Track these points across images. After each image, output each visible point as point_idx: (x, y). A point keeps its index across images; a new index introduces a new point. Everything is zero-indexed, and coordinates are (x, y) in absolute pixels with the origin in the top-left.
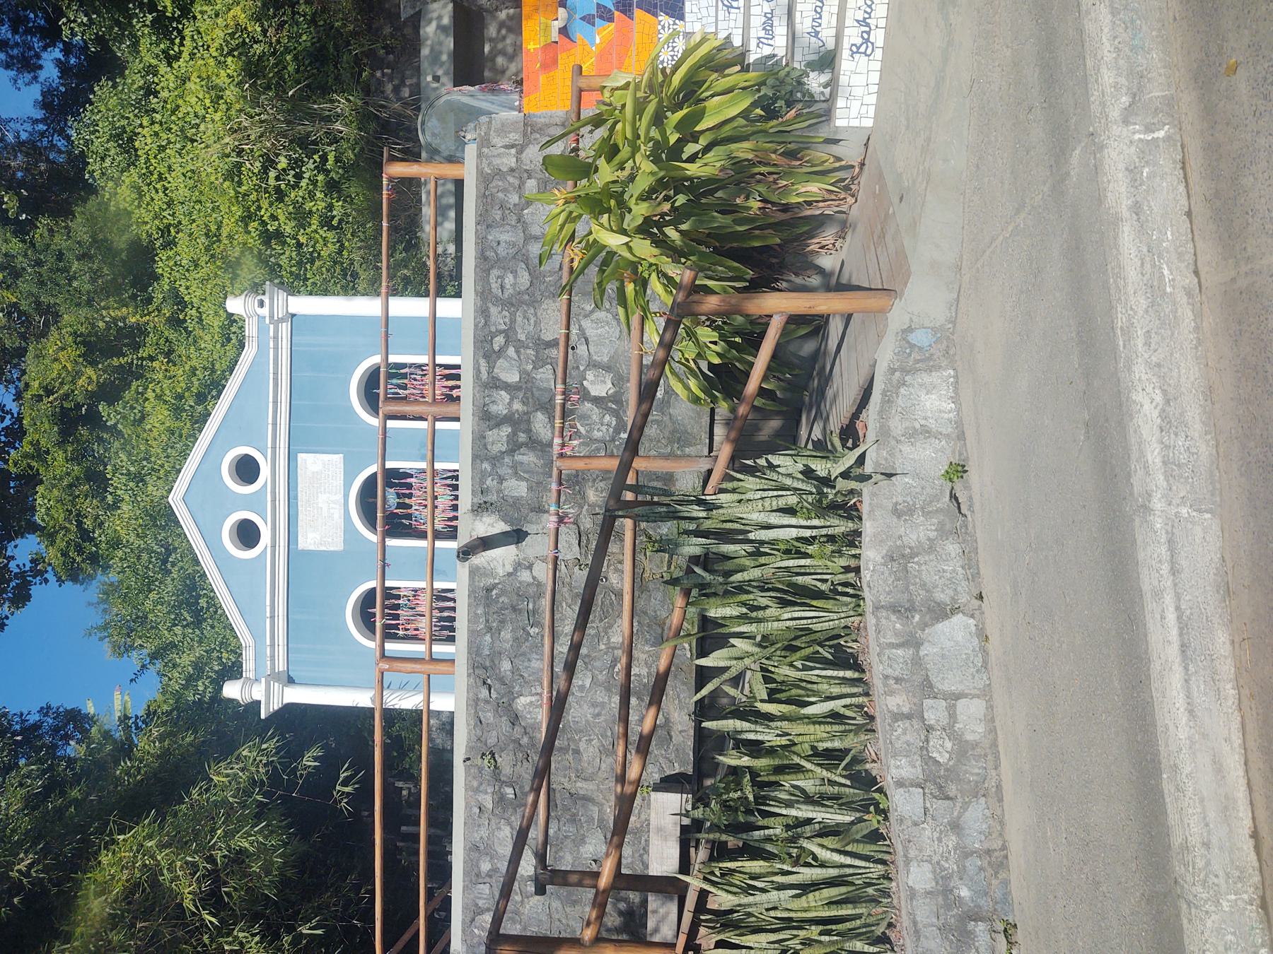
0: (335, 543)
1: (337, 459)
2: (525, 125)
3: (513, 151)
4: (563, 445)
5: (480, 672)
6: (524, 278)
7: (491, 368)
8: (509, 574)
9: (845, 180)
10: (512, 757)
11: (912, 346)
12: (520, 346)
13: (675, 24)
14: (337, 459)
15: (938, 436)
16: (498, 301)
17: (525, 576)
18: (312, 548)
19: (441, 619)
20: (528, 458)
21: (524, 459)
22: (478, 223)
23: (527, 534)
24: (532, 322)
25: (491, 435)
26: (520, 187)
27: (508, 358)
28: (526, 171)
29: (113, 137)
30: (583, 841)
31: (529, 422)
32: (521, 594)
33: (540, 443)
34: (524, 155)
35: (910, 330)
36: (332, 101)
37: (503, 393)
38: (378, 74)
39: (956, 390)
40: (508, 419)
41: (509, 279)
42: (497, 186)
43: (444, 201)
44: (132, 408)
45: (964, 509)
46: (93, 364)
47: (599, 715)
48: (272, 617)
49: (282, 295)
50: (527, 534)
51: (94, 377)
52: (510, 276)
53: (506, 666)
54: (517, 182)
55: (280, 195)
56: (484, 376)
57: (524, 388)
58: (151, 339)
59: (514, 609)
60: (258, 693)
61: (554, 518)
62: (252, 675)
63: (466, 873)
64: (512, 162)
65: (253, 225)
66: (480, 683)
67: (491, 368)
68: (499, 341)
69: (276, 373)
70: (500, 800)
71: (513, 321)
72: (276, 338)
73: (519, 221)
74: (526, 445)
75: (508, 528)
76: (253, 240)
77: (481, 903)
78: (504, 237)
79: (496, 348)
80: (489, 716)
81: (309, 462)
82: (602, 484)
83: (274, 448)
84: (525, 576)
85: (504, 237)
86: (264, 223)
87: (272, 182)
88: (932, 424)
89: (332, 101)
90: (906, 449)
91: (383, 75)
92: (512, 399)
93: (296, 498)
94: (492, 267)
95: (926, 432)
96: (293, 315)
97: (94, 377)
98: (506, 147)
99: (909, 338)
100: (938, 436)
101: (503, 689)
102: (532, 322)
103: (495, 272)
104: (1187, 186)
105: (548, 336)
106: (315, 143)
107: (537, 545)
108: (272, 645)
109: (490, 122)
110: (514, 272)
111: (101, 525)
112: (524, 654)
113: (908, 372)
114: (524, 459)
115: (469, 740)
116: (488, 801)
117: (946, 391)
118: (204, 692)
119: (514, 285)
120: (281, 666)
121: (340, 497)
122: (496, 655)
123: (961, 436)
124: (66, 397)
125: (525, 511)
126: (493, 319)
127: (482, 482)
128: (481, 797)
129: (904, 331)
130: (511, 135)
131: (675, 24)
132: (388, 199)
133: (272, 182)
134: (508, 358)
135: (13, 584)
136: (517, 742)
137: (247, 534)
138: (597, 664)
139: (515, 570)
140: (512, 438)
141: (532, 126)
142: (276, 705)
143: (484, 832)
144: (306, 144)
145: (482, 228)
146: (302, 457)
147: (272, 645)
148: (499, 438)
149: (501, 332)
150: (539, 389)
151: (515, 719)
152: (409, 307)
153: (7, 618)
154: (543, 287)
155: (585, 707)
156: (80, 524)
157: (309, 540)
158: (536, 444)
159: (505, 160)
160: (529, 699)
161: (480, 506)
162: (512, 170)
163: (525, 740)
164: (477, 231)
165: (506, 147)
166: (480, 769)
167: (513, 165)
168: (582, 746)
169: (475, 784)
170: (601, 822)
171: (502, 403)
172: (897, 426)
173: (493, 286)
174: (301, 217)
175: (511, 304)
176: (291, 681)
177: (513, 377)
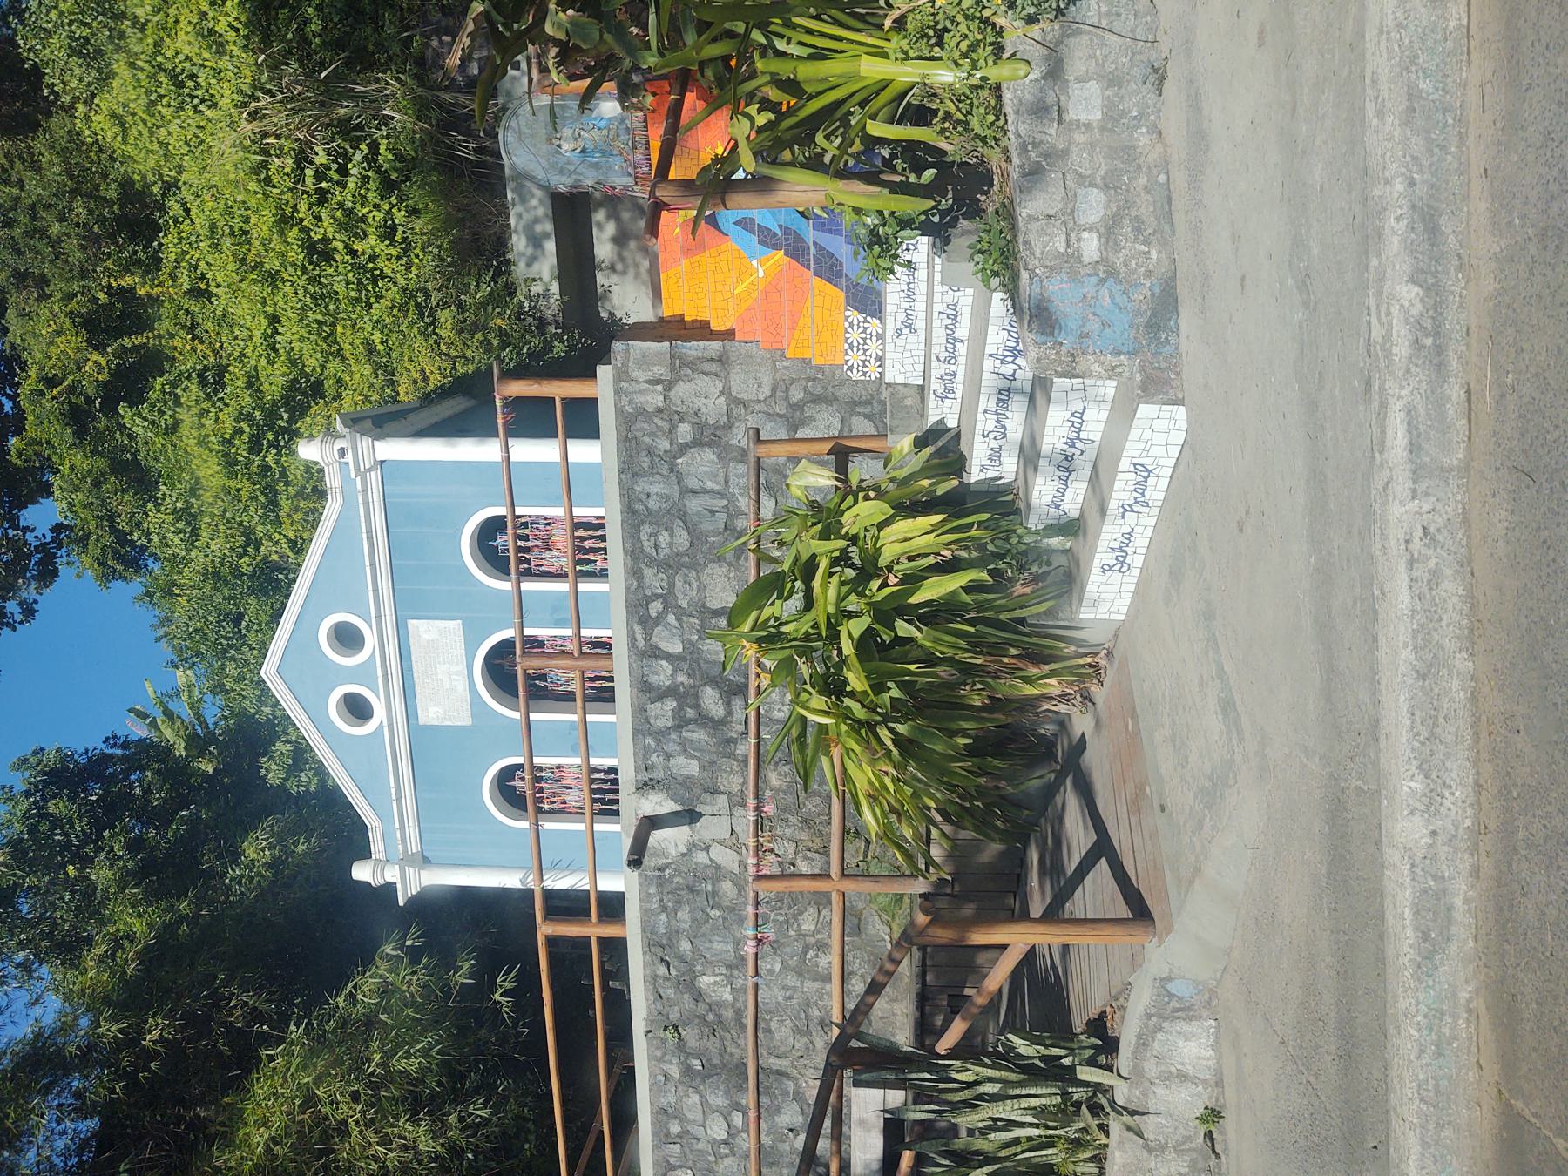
0: (463, 718)
1: (455, 626)
2: (672, 357)
3: (659, 388)
4: (758, 865)
5: (659, 950)
6: (682, 538)
7: (648, 636)
8: (684, 855)
9: (1089, 673)
10: (696, 1031)
11: (1171, 995)
12: (681, 614)
13: (866, 321)
14: (455, 626)
15: (1194, 1080)
16: (652, 562)
17: (701, 857)
18: (436, 723)
19: (593, 792)
20: (698, 735)
21: (695, 736)
22: (621, 472)
23: (701, 815)
24: (695, 586)
25: (654, 709)
26: (671, 432)
27: (667, 626)
28: (679, 414)
29: (73, 52)
30: (778, 1111)
31: (696, 696)
32: (698, 875)
33: (711, 719)
34: (672, 393)
35: (1169, 979)
36: (377, 80)
37: (664, 663)
38: (435, 43)
39: (1217, 1039)
40: (672, 691)
41: (664, 538)
42: (643, 429)
43: (538, 228)
44: (162, 413)
45: (1218, 1149)
46: (100, 348)
47: (790, 998)
48: (399, 799)
49: (366, 441)
50: (701, 815)
51: (104, 363)
52: (666, 534)
53: (685, 945)
54: (666, 426)
55: (322, 197)
56: (641, 644)
57: (689, 658)
58: (167, 310)
59: (691, 889)
60: (391, 875)
61: (753, 943)
62: (382, 856)
63: (654, 1134)
64: (659, 401)
65: (294, 232)
66: (657, 961)
67: (648, 636)
68: (656, 607)
69: (369, 532)
70: (687, 1071)
71: (672, 585)
72: (364, 491)
73: (672, 470)
74: (694, 721)
75: (679, 808)
76: (296, 255)
77: (672, 1160)
78: (655, 489)
79: (654, 614)
80: (669, 992)
81: (423, 631)
82: (786, 769)
83: (378, 617)
84: (701, 857)
85: (655, 489)
86: (305, 230)
87: (309, 180)
88: (1189, 1070)
89: (377, 80)
90: (1160, 1091)
91: (441, 42)
92: (675, 671)
93: (411, 669)
94: (643, 522)
95: (1183, 1077)
96: (382, 462)
97: (104, 363)
98: (649, 382)
99: (1168, 987)
100: (1194, 1080)
101: (683, 968)
102: (695, 586)
103: (646, 529)
104: (1470, 421)
105: (715, 604)
106: (359, 127)
107: (713, 827)
108: (402, 828)
109: (627, 351)
110: (670, 530)
111: (138, 525)
112: (704, 935)
113: (1165, 1019)
114: (695, 736)
115: (649, 1014)
116: (674, 1071)
117: (1206, 1040)
118: (309, 783)
119: (670, 545)
120: (414, 847)
121: (463, 667)
122: (673, 934)
123: (1219, 1083)
124: (72, 389)
125: (697, 791)
126: (647, 581)
127: (646, 756)
128: (666, 1067)
129: (1162, 979)
130: (655, 369)
131: (866, 321)
132: (505, 423)
133: (309, 180)
134: (667, 626)
135: (35, 559)
136: (702, 1018)
137: (357, 708)
138: (788, 950)
139: (689, 850)
140: (678, 713)
141: (680, 358)
142: (413, 890)
143: (671, 1098)
144: (348, 130)
145: (627, 477)
146: (413, 624)
147: (402, 828)
148: (663, 713)
149: (658, 596)
150: (706, 661)
151: (698, 996)
152: (529, 451)
153: (36, 602)
154: (705, 548)
155: (776, 990)
156: (114, 530)
157: (430, 714)
158: (704, 720)
159: (649, 398)
160: (712, 979)
161: (645, 784)
162: (660, 410)
163: (711, 1017)
164: (621, 481)
165: (649, 382)
166: (664, 1041)
167: (661, 404)
168: (774, 1025)
169: (659, 1054)
170: (798, 1097)
171: (663, 674)
172: (1151, 1068)
173: (646, 544)
174: (351, 223)
175: (669, 565)
176: (425, 861)
177: (676, 648)
